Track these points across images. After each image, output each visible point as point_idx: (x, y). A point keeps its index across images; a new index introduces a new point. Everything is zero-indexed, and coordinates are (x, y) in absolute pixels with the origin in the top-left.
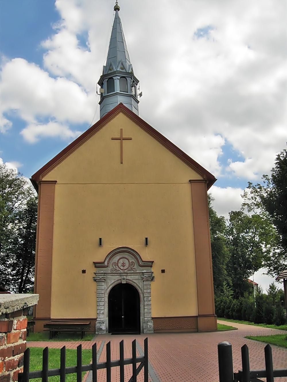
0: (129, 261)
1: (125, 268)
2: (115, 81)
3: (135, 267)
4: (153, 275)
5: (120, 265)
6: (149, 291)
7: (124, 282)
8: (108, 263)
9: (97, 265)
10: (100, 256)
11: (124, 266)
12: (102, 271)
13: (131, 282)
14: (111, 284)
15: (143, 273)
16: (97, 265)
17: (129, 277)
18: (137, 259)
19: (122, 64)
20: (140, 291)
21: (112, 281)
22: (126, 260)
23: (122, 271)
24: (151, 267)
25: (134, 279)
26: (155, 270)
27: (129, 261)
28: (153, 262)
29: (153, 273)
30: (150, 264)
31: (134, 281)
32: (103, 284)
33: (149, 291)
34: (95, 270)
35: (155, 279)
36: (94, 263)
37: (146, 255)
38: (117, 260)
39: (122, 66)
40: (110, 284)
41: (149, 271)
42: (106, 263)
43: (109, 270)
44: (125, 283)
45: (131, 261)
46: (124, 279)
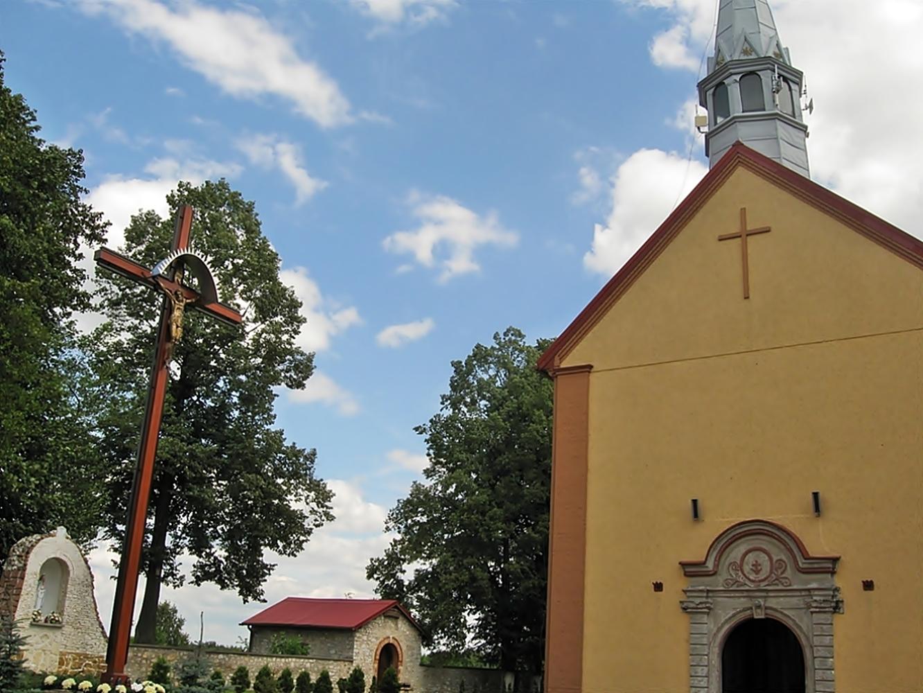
0: (771, 559)
1: (762, 576)
2: (729, 88)
3: (789, 573)
4: (840, 597)
5: (747, 568)
6: (827, 640)
7: (759, 615)
8: (716, 566)
9: (688, 570)
10: (696, 546)
11: (757, 572)
12: (702, 584)
13: (779, 615)
14: (726, 621)
15: (809, 590)
16: (688, 570)
17: (772, 603)
18: (790, 550)
19: (746, 40)
20: (803, 641)
21: (729, 611)
22: (763, 555)
23: (752, 586)
24: (833, 573)
25: (786, 608)
26: (846, 583)
27: (771, 559)
28: (835, 560)
29: (837, 590)
30: (830, 565)
31: (786, 612)
32: (705, 618)
33: (827, 640)
34: (684, 583)
35: (846, 607)
36: (683, 565)
37: (819, 542)
38: (740, 556)
39: (746, 45)
40: (723, 620)
41: (827, 585)
42: (710, 565)
43: (719, 583)
44: (763, 617)
45: (775, 558)
46: (759, 607)
